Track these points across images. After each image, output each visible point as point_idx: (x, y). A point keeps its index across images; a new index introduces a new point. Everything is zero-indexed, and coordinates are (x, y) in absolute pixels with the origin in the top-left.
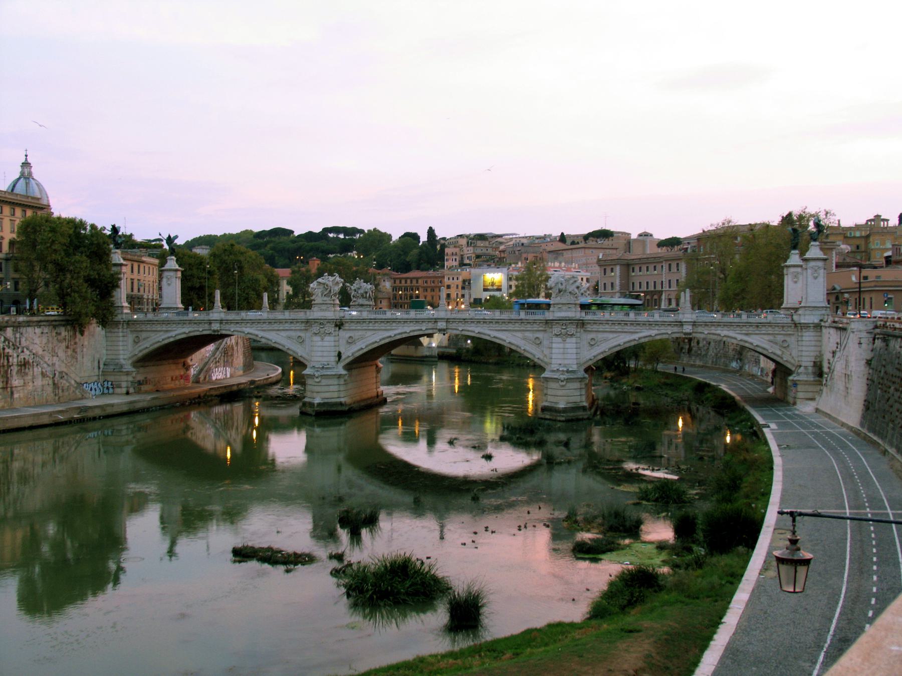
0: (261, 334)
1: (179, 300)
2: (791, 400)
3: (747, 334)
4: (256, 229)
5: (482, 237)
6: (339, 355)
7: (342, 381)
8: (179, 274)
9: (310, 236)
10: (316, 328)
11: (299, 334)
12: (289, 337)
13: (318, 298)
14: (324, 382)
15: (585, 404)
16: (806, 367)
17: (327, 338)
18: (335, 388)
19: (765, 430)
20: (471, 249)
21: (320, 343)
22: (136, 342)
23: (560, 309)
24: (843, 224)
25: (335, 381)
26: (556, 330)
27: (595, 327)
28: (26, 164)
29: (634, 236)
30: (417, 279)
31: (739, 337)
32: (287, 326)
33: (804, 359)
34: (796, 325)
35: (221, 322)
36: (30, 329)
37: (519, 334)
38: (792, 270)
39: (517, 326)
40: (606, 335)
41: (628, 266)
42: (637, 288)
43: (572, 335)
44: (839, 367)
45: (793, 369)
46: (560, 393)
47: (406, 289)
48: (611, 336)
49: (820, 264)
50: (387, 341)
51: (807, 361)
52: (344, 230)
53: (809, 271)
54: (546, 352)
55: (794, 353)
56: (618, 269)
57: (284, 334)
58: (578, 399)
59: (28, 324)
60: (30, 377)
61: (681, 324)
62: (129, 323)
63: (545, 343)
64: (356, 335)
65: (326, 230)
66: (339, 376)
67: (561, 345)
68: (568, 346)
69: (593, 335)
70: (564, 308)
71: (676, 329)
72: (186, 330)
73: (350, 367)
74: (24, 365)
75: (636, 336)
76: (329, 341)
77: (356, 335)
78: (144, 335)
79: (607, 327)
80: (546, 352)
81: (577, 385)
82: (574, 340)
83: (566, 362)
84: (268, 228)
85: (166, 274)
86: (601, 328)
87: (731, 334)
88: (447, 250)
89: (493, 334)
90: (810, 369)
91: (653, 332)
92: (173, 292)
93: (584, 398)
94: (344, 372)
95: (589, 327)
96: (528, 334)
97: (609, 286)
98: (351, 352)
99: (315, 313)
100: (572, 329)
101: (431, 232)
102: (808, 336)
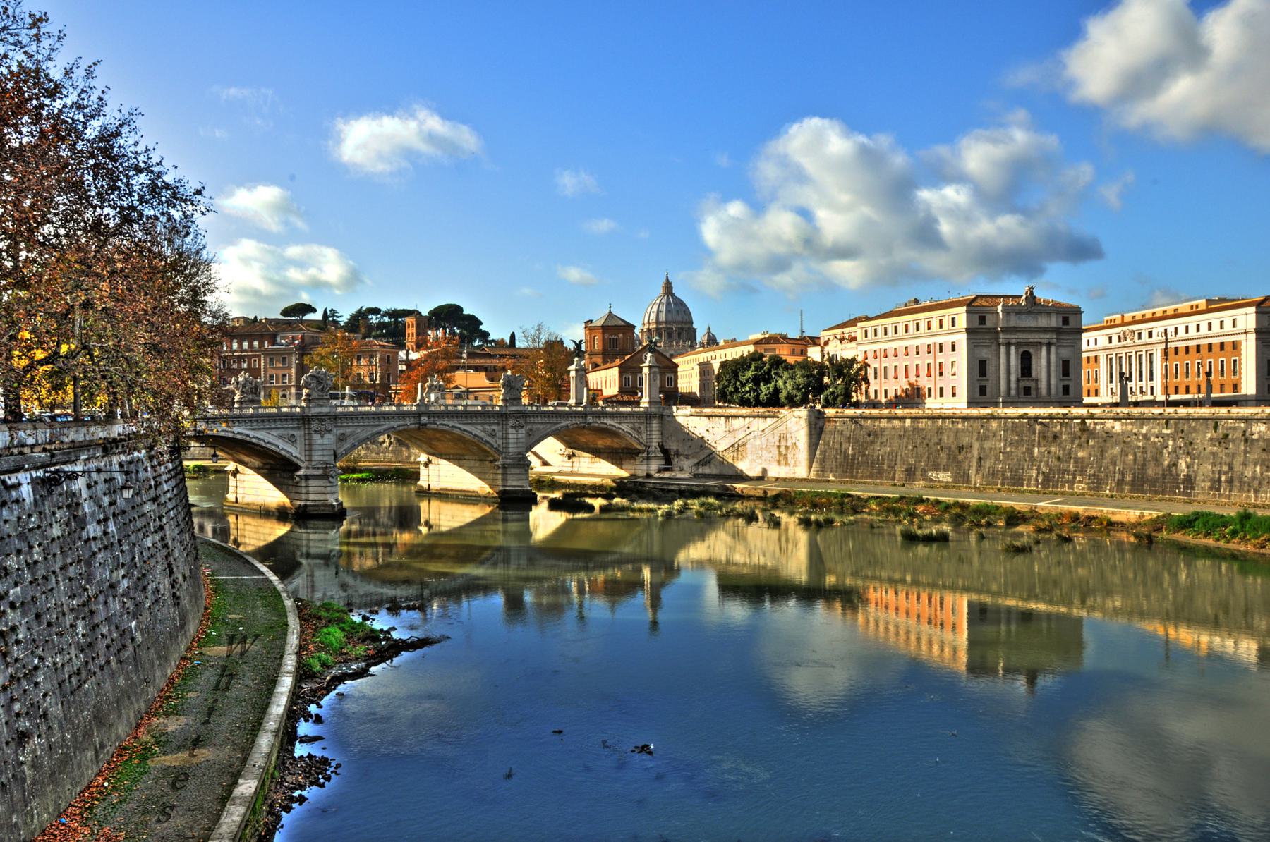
0: (252, 433)
10: (314, 426)
11: (291, 432)
12: (281, 437)
17: (327, 436)
21: (320, 442)
26: (511, 423)
32: (279, 424)
34: (647, 416)
51: (655, 442)
54: (500, 442)
57: (275, 433)
64: (349, 431)
69: (529, 427)
82: (523, 431)
96: (487, 427)
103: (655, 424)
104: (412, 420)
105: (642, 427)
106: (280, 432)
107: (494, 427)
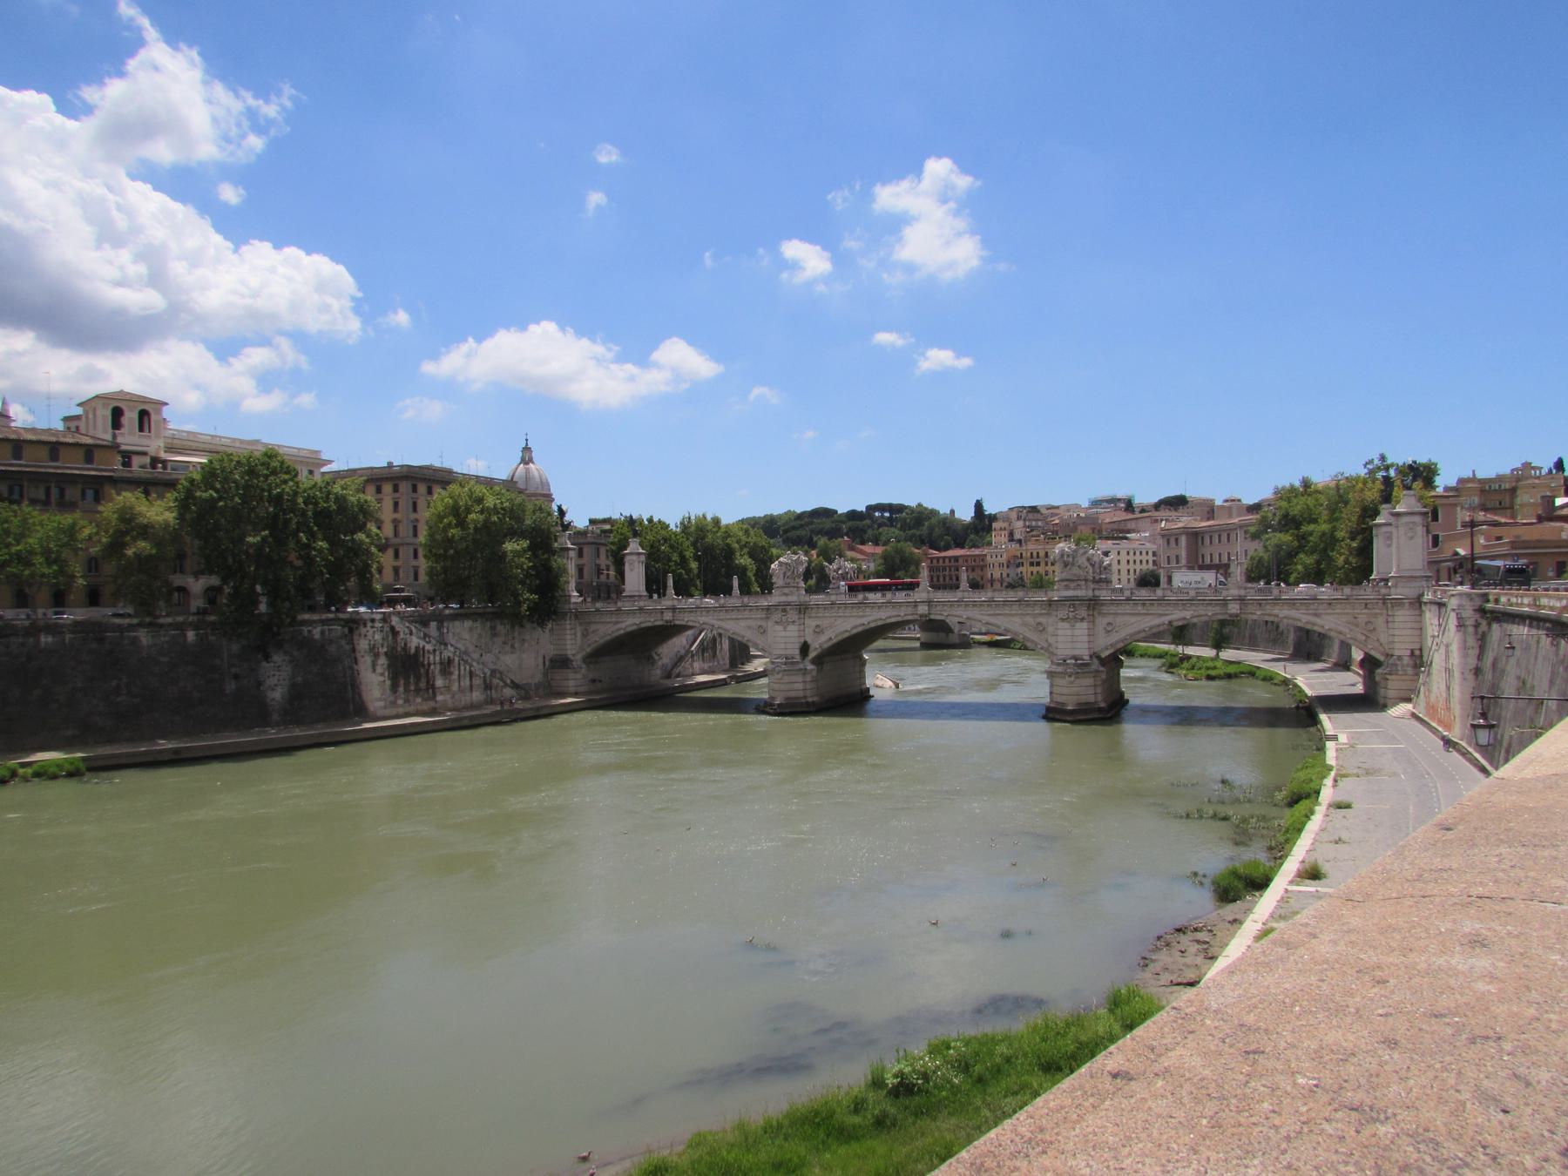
0: (717, 623)
1: (643, 588)
2: (1381, 701)
3: (1316, 615)
4: (799, 511)
5: (1034, 509)
6: (805, 649)
7: (808, 678)
8: (643, 558)
9: (853, 515)
10: (777, 616)
13: (778, 581)
14: (786, 679)
15: (1103, 705)
16: (1400, 658)
17: (790, 627)
18: (800, 686)
19: (1330, 745)
20: (1020, 524)
22: (584, 635)
23: (1067, 588)
24: (1480, 475)
25: (800, 679)
26: (1062, 613)
27: (1113, 609)
28: (527, 449)
29: (1219, 502)
30: (956, 559)
31: (1305, 618)
32: (746, 614)
33: (1397, 646)
34: (1384, 600)
35: (674, 609)
36: (457, 623)
37: (1017, 620)
38: (1384, 529)
39: (1015, 609)
40: (1126, 618)
41: (1195, 536)
42: (1208, 561)
43: (1082, 619)
44: (1438, 660)
45: (1382, 658)
46: (1065, 691)
47: (944, 569)
48: (1133, 619)
49: (1418, 519)
50: (860, 629)
51: (1402, 649)
52: (890, 508)
53: (1402, 530)
55: (1384, 638)
56: (1183, 539)
57: (743, 623)
58: (1091, 699)
59: (455, 617)
60: (455, 677)
61: (1225, 602)
62: (578, 615)
63: (1050, 629)
65: (869, 508)
66: (805, 672)
67: (1069, 632)
68: (1077, 632)
69: (1109, 619)
70: (1072, 585)
71: (1218, 609)
72: (637, 621)
73: (818, 661)
74: (446, 667)
75: (1166, 619)
76: (793, 630)
77: (825, 623)
78: (593, 627)
79: (1128, 608)
80: (1051, 640)
81: (1089, 681)
82: (1085, 625)
83: (1077, 652)
84: (809, 508)
85: (628, 558)
86: (1120, 610)
87: (1293, 613)
88: (994, 525)
89: (986, 619)
90: (1406, 660)
91: (1188, 614)
92: (635, 578)
93: (1100, 698)
94: (810, 667)
95: (1105, 609)
96: (1029, 620)
97: (1173, 559)
98: (818, 644)
99: (776, 598)
100: (1083, 612)
101: (979, 506)
102: (1403, 616)
103: (1403, 616)
104: (910, 610)
105: (1381, 621)
106: (750, 622)
107: (1040, 619)
